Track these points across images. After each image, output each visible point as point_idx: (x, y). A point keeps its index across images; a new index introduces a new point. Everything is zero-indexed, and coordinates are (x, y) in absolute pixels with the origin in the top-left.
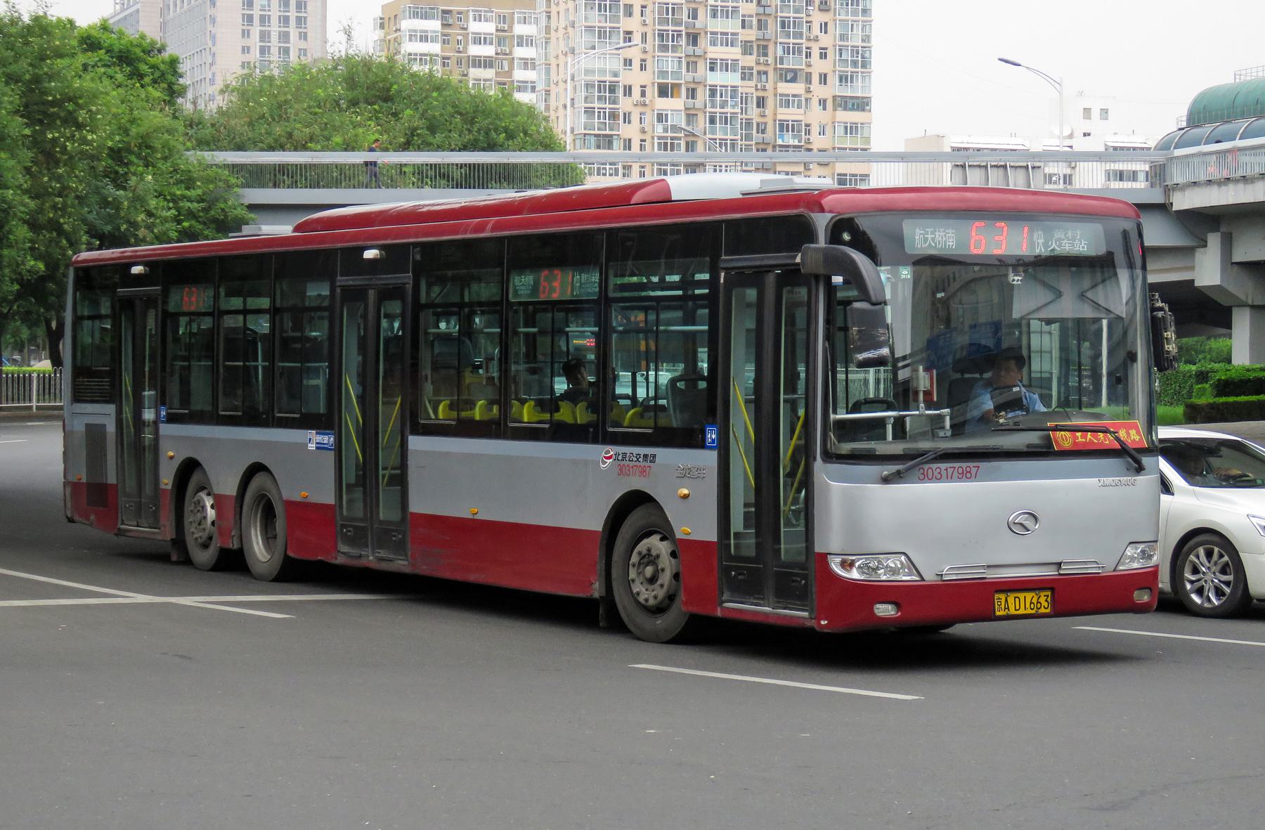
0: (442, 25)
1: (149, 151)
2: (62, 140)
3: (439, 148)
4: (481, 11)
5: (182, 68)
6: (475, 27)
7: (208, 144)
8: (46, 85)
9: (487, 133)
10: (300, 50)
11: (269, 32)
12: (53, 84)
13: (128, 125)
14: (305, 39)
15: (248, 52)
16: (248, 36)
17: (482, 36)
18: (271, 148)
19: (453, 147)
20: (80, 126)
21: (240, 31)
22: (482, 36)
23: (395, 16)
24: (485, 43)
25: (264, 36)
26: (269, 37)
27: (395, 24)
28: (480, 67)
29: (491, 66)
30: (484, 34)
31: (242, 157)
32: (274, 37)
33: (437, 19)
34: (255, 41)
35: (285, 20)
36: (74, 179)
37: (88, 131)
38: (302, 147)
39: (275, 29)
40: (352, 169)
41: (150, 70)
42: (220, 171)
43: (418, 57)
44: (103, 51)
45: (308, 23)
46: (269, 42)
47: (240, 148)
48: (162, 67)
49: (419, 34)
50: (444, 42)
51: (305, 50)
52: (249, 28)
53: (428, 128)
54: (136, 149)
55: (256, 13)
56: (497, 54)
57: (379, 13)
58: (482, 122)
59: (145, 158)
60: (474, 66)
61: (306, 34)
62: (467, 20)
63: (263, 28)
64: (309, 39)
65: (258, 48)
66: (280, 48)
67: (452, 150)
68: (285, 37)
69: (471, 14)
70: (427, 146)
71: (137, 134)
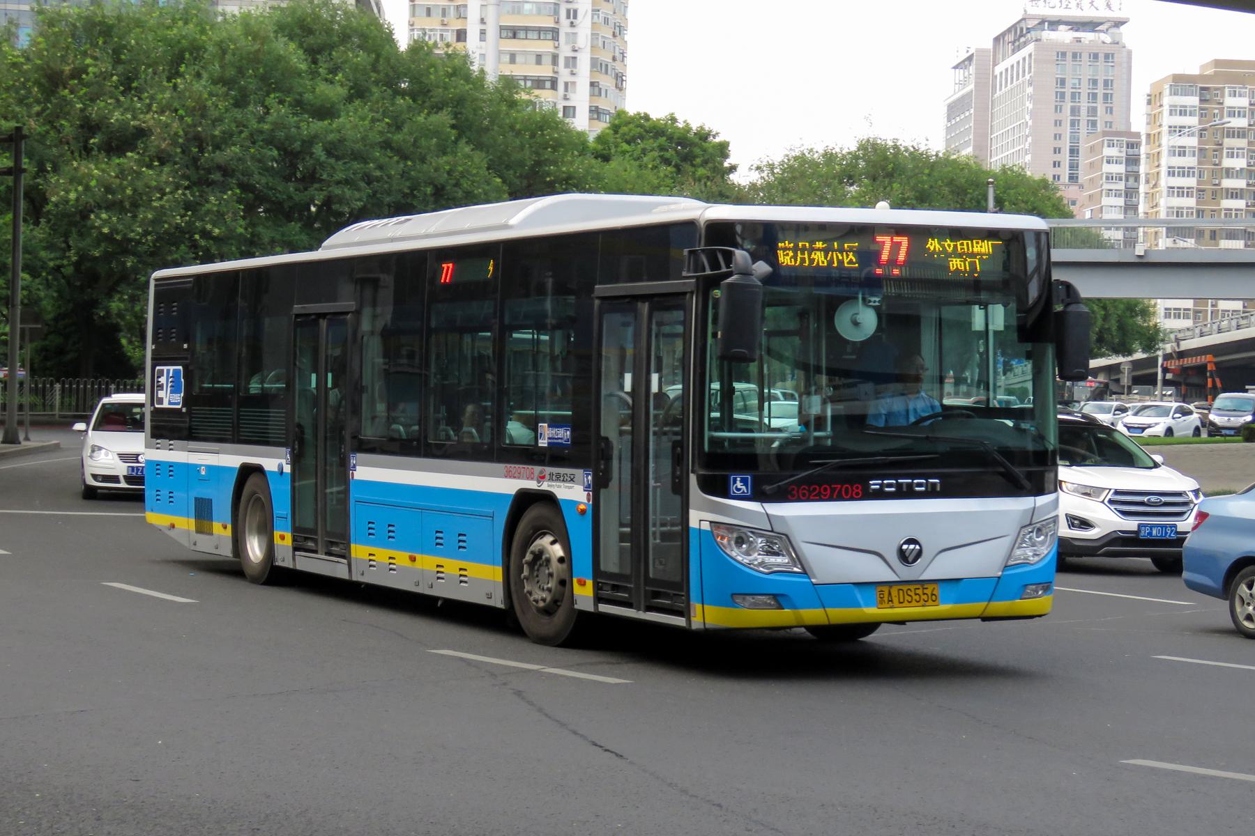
0: (1201, 101)
4: (1235, 88)
6: (1229, 101)
10: (1106, 122)
11: (1080, 107)
14: (1111, 113)
15: (1060, 125)
16: (1060, 112)
17: (1237, 110)
21: (1054, 107)
22: (1237, 110)
23: (1160, 93)
24: (1239, 116)
25: (1075, 111)
26: (1079, 111)
27: (1160, 101)
28: (1234, 137)
29: (1244, 136)
30: (1239, 108)
32: (1084, 111)
33: (1196, 96)
34: (1066, 115)
35: (1094, 96)
39: (1084, 105)
43: (1178, 129)
45: (1114, 99)
46: (1079, 116)
49: (1178, 109)
50: (1201, 115)
51: (1111, 122)
52: (1061, 103)
55: (1068, 91)
56: (1250, 125)
57: (1149, 92)
60: (1228, 136)
61: (1111, 108)
62: (1223, 96)
63: (1073, 104)
64: (1114, 113)
65: (1069, 121)
66: (1088, 120)
68: (1092, 111)
69: (1227, 90)
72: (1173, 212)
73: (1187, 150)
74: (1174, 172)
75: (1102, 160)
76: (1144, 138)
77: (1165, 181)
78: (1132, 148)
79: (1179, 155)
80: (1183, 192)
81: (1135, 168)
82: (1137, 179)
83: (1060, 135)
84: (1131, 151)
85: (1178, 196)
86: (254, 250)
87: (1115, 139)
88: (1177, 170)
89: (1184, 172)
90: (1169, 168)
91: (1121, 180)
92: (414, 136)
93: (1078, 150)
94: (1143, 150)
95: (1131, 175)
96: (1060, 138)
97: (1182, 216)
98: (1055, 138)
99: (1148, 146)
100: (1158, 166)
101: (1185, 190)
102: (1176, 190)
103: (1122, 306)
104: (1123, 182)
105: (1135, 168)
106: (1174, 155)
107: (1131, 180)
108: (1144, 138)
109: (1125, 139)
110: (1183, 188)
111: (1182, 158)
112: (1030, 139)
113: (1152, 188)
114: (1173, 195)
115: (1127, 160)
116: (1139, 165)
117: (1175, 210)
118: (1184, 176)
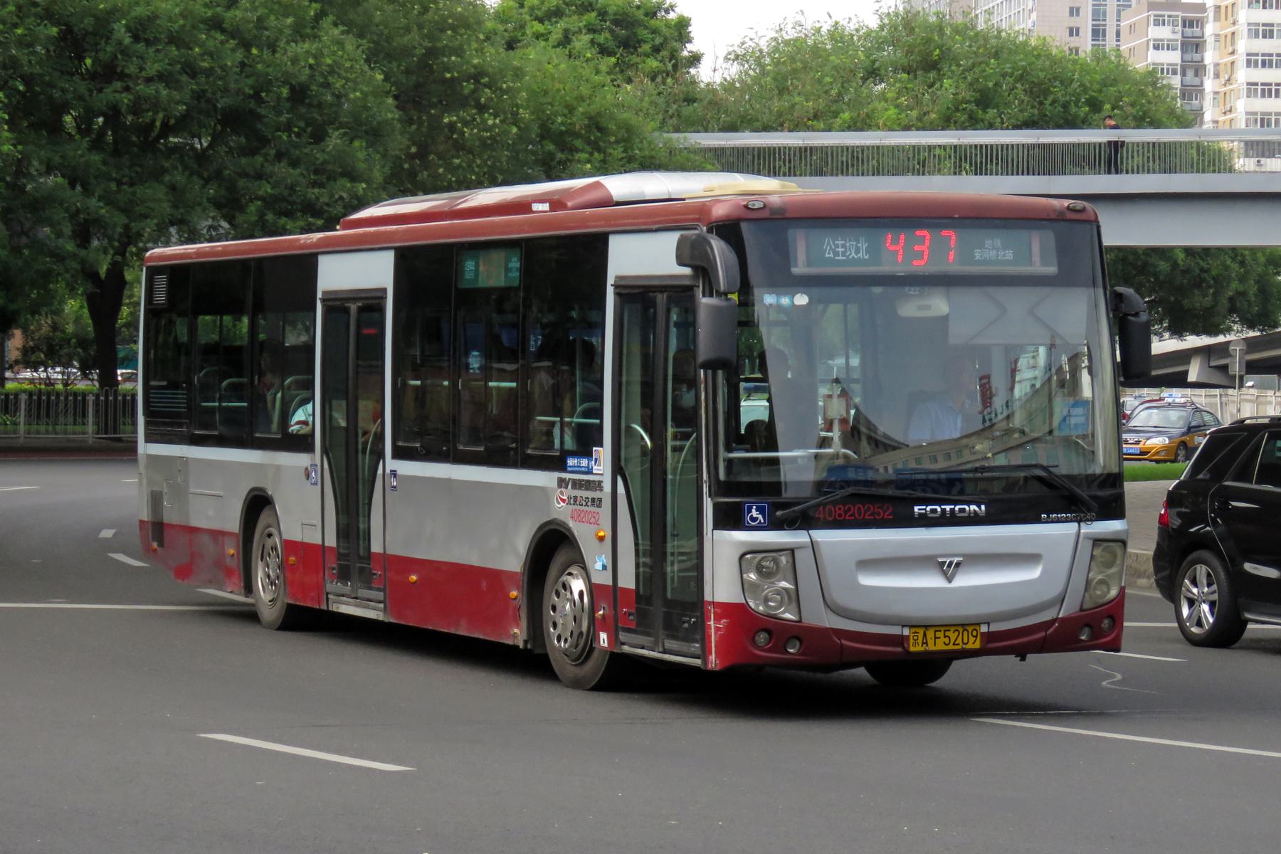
1: (599, 134)
2: (459, 125)
3: (991, 126)
5: (694, 30)
7: (693, 124)
8: (445, 59)
9: (1065, 106)
12: (453, 58)
13: (575, 103)
18: (766, 128)
19: (1005, 125)
20: (482, 108)
31: (722, 140)
36: (476, 169)
37: (491, 114)
38: (796, 127)
40: (845, 153)
41: (650, 36)
42: (692, 156)
44: (594, 14)
47: (732, 128)
48: (665, 31)
53: (978, 103)
54: (583, 132)
58: (1058, 91)
59: (596, 142)
67: (1007, 128)
70: (973, 123)
71: (582, 114)
72: (1256, 120)
73: (1275, 29)
74: (1256, 62)
75: (1148, 44)
76: (1211, 14)
77: (1243, 75)
78: (1191, 26)
79: (1264, 37)
80: (1270, 91)
81: (1197, 57)
82: (1199, 69)
83: (1078, 9)
84: (1188, 31)
85: (1263, 96)
86: (25, 181)
87: (1167, 13)
88: (1260, 58)
89: (1271, 62)
90: (1248, 55)
91: (1175, 73)
92: (259, 14)
93: (1104, 31)
94: (1210, 29)
95: (1190, 67)
96: (1078, 14)
97: (1269, 125)
98: (1071, 14)
99: (1218, 24)
100: (1233, 53)
101: (1274, 88)
102: (1259, 88)
103: (1262, 259)
104: (1178, 78)
105: (1197, 57)
106: (1257, 36)
107: (1190, 73)
108: (1211, 14)
109: (1180, 14)
110: (1271, 84)
111: (1268, 41)
112: (1034, 16)
113: (1225, 85)
114: (1256, 96)
115: (1183, 44)
116: (1203, 51)
117: (1259, 117)
118: (1271, 66)
